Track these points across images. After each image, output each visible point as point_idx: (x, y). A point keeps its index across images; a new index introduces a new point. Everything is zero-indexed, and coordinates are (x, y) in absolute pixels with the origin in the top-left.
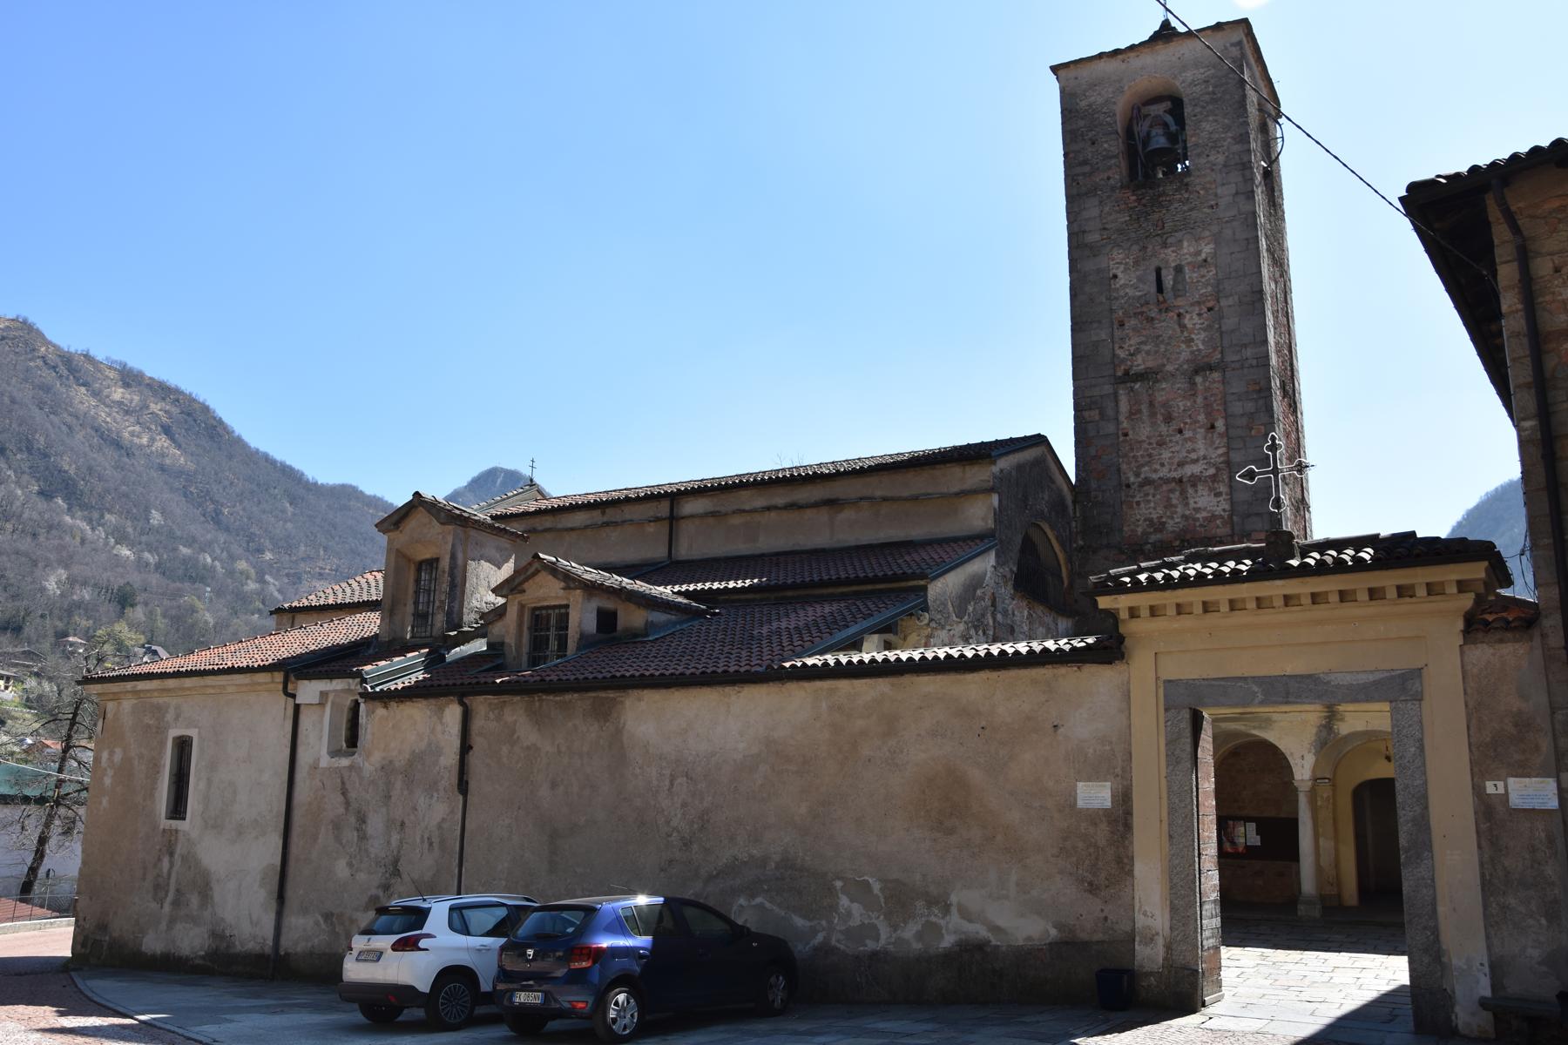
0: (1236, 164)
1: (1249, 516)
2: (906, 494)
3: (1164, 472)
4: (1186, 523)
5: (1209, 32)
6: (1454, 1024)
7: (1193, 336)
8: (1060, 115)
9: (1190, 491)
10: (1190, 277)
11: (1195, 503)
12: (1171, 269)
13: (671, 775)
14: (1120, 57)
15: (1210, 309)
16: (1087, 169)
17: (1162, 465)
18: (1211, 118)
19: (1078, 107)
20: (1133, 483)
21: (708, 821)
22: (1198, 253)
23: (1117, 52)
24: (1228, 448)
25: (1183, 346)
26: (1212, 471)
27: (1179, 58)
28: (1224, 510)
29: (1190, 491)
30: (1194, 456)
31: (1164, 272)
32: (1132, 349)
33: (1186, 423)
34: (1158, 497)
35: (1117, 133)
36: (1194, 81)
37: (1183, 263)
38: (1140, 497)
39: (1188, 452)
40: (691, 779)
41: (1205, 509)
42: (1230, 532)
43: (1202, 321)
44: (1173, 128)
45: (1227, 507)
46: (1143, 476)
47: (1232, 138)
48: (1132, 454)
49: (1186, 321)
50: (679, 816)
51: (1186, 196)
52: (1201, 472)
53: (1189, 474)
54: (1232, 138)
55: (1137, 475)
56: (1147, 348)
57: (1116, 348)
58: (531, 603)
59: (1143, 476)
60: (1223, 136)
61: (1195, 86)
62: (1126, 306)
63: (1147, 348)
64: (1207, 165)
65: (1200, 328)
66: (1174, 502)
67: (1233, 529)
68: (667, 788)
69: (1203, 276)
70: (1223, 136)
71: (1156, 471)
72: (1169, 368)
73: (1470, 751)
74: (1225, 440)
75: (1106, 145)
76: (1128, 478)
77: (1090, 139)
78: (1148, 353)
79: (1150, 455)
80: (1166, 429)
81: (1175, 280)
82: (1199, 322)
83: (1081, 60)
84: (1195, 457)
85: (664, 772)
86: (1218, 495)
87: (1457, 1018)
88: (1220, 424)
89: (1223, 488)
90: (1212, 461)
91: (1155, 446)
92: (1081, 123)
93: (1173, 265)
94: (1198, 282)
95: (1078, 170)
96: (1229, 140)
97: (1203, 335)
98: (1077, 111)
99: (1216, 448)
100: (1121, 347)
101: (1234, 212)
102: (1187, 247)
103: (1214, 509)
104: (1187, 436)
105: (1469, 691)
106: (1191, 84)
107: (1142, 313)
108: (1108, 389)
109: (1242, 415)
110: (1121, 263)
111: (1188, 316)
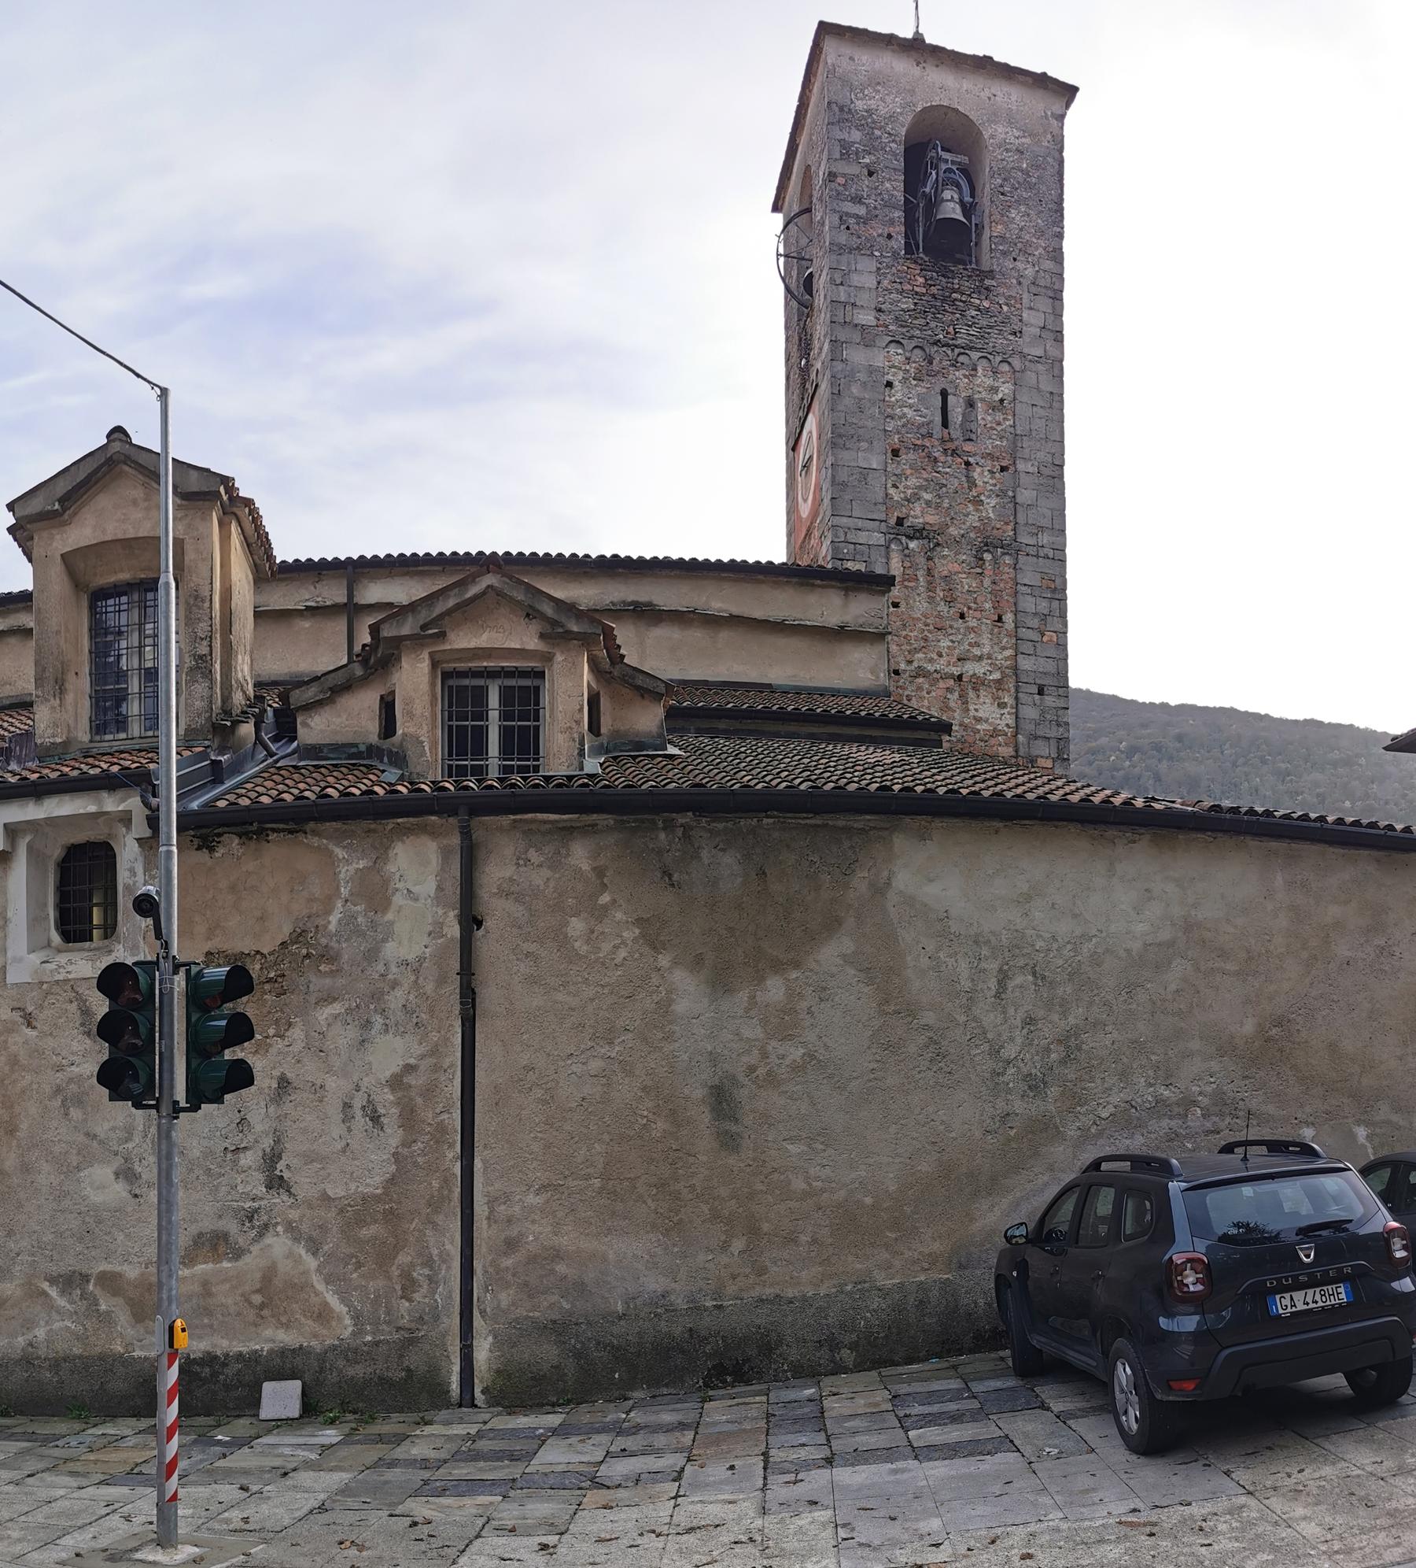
1: (1036, 738)
2: (758, 614)
3: (941, 665)
4: (965, 733)
5: (1030, 80)
7: (983, 498)
9: (971, 694)
10: (983, 419)
11: (976, 710)
12: (961, 400)
13: (1000, 970)
15: (1003, 469)
17: (940, 655)
20: (905, 671)
21: (1079, 1049)
22: (994, 390)
24: (1016, 650)
25: (971, 508)
26: (997, 676)
28: (1007, 725)
29: (971, 694)
30: (977, 652)
31: (951, 399)
32: (909, 492)
33: (969, 608)
34: (934, 694)
37: (976, 396)
38: (913, 691)
39: (970, 644)
40: (1044, 978)
41: (986, 721)
42: (1013, 753)
43: (994, 481)
45: (1011, 722)
46: (915, 664)
48: (904, 633)
49: (976, 475)
50: (1019, 1040)
51: (986, 304)
52: (984, 674)
53: (971, 673)
55: (910, 662)
56: (927, 496)
57: (889, 485)
58: (448, 662)
59: (915, 664)
61: (1007, 150)
62: (903, 430)
63: (927, 496)
65: (991, 490)
66: (952, 704)
67: (1017, 751)
68: (993, 993)
69: (999, 424)
71: (931, 660)
72: (953, 531)
74: (1014, 641)
76: (898, 663)
77: (867, 165)
78: (928, 503)
79: (926, 640)
80: (946, 610)
82: (991, 481)
83: (865, 32)
84: (979, 653)
85: (984, 965)
86: (1002, 705)
88: (1009, 618)
89: (1008, 699)
90: (997, 662)
91: (931, 627)
93: (963, 395)
94: (993, 428)
96: (1041, 250)
97: (993, 502)
99: (1004, 648)
100: (895, 486)
102: (983, 379)
103: (998, 722)
104: (971, 624)
107: (924, 447)
108: (878, 538)
109: (1035, 614)
111: (978, 470)
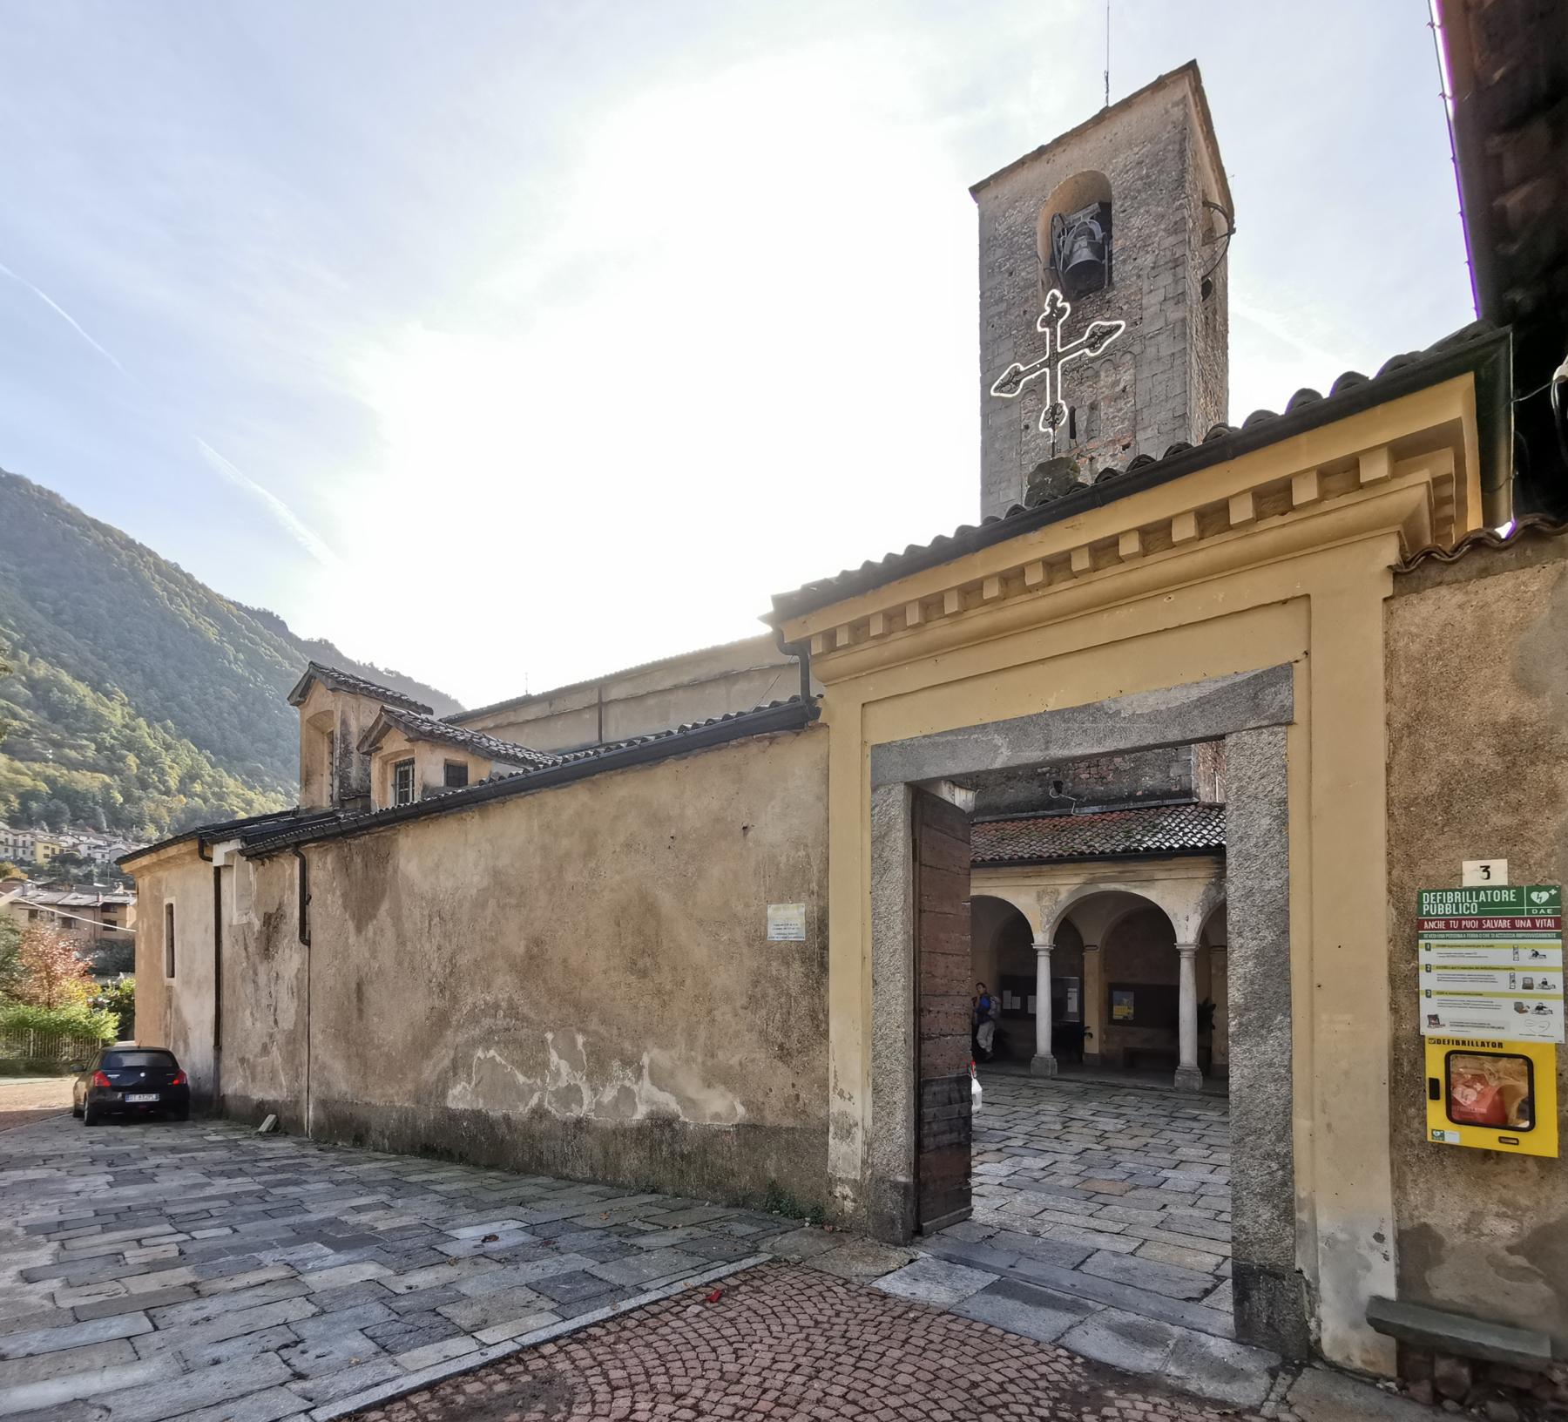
0: (1166, 263)
6: (1312, 1338)
8: (978, 248)
14: (1045, 157)
16: (1003, 306)
18: (1142, 211)
19: (996, 233)
22: (1116, 383)
23: (1041, 151)
27: (1111, 141)
31: (1077, 413)
35: (1038, 257)
36: (1126, 166)
44: (1099, 235)
47: (1165, 230)
54: (1165, 230)
60: (1154, 229)
64: (1133, 272)
70: (1154, 229)
73: (1390, 816)
75: (1023, 274)
77: (1007, 270)
81: (1088, 420)
87: (1319, 1326)
92: (999, 252)
94: (1114, 417)
95: (994, 310)
98: (995, 238)
101: (1160, 323)
105: (1397, 692)
106: (1121, 172)
110: (1034, 411)
111: (1101, 459)
